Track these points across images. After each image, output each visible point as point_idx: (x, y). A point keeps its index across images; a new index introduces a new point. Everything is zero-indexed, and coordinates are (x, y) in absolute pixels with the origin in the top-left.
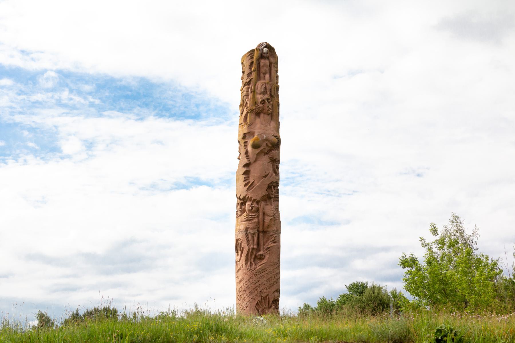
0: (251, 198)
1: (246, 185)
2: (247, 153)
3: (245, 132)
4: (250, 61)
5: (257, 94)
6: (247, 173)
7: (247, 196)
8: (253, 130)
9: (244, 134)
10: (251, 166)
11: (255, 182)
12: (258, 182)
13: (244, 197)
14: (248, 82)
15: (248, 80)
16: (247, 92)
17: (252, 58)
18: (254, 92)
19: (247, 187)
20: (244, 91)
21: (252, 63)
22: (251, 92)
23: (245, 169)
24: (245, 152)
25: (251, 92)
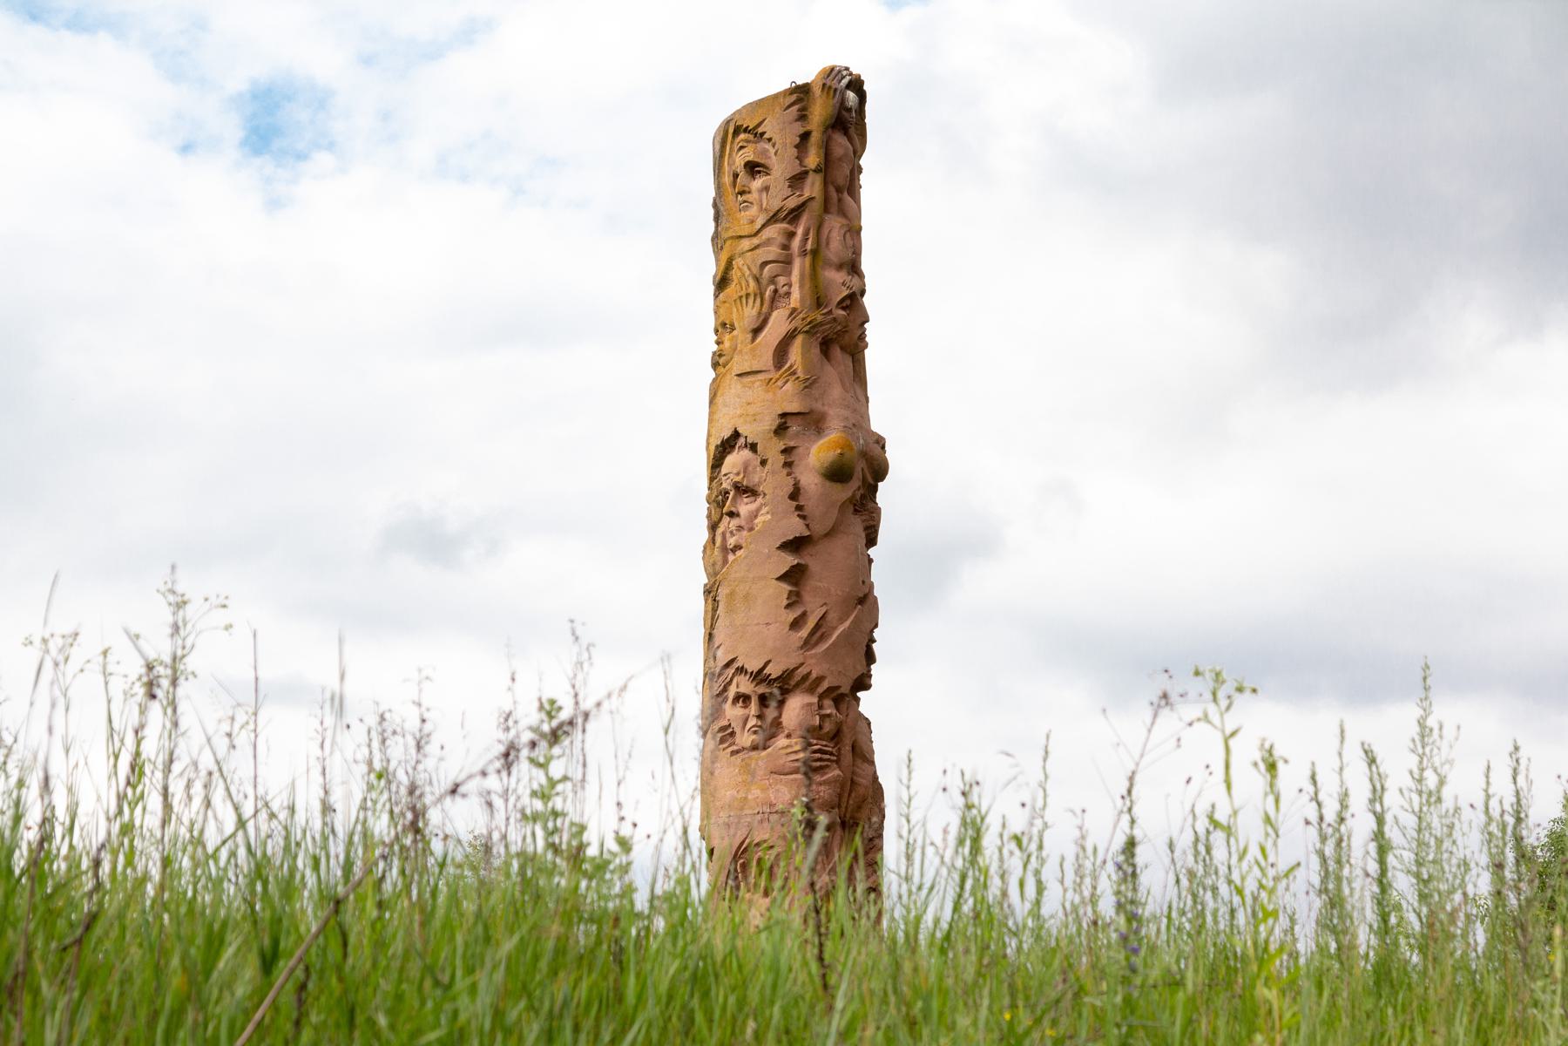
0: (820, 679)
1: (796, 624)
2: (795, 495)
3: (793, 407)
4: (799, 129)
6: (794, 576)
7: (802, 671)
8: (818, 406)
9: (784, 415)
10: (810, 550)
11: (830, 617)
13: (786, 676)
14: (793, 211)
15: (792, 203)
16: (786, 247)
17: (802, 117)
18: (815, 253)
19: (804, 633)
20: (768, 242)
21: (805, 136)
22: (804, 253)
23: (789, 560)
25: (804, 253)
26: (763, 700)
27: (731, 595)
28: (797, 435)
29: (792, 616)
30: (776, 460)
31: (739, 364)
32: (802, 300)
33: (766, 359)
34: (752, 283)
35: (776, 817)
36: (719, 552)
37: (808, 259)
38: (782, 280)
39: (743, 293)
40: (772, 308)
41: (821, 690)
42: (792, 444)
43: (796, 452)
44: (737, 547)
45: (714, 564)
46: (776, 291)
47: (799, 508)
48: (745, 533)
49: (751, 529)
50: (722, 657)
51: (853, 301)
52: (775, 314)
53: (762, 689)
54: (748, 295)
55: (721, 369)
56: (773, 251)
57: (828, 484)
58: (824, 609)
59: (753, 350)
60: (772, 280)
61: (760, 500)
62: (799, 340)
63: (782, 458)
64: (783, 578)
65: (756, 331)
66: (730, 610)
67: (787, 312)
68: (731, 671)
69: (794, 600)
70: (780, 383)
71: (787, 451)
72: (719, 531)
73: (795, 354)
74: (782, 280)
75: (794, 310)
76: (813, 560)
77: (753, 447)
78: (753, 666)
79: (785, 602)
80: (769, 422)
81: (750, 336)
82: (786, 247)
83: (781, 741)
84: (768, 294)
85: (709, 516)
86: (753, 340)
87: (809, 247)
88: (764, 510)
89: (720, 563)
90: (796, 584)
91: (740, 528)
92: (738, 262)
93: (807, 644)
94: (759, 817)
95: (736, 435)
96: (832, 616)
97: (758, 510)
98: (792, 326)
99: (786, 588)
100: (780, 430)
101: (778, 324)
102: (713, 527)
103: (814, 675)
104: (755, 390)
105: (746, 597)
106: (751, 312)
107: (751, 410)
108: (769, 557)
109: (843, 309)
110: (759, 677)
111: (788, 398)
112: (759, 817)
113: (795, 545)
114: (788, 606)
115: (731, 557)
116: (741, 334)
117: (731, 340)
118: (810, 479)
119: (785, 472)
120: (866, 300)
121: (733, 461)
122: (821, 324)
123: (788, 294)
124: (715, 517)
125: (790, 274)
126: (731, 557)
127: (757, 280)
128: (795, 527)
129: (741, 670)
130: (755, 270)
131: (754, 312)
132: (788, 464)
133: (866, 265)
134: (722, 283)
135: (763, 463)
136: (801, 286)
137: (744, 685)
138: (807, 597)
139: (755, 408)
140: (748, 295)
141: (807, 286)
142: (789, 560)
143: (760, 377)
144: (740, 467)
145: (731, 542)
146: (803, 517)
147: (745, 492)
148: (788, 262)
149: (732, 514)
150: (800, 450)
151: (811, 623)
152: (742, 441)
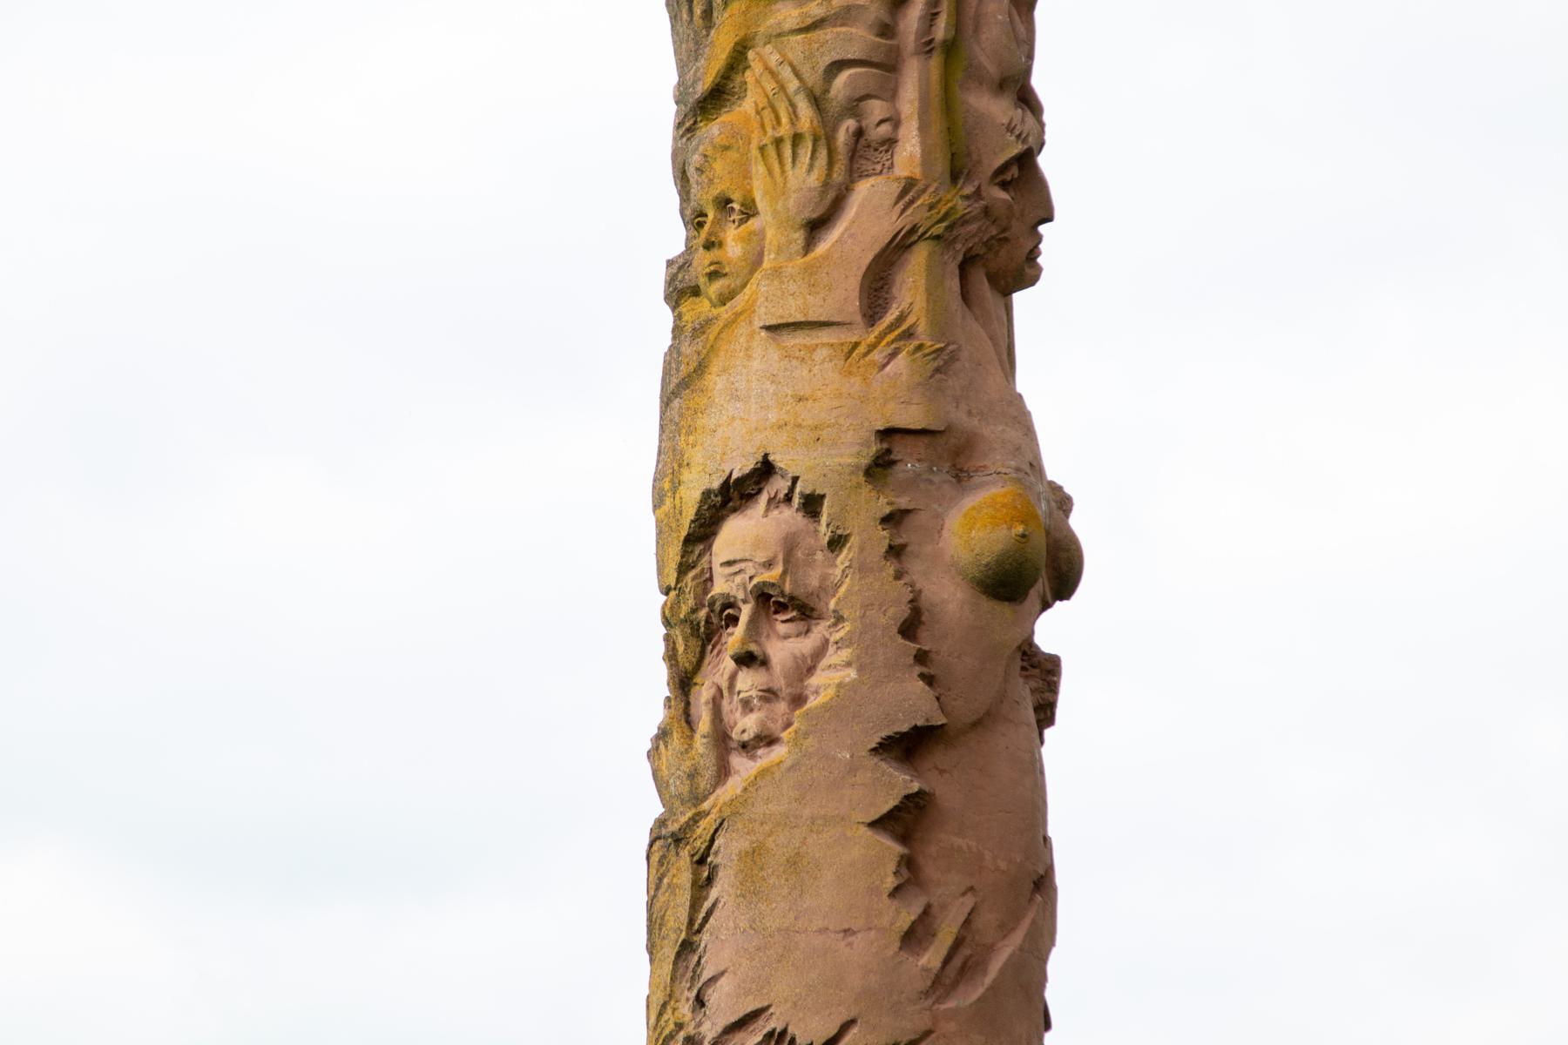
1: (914, 937)
2: (909, 628)
5: (975, 76)
6: (905, 821)
8: (959, 417)
9: (887, 434)
10: (939, 757)
11: (980, 922)
12: (1005, 929)
16: (886, 30)
18: (951, 48)
19: (932, 958)
22: (927, 48)
23: (899, 782)
24: (904, 612)
25: (927, 48)
27: (754, 855)
28: (912, 483)
29: (907, 917)
30: (867, 537)
31: (769, 298)
32: (926, 154)
33: (844, 295)
34: (805, 111)
36: (698, 743)
37: (936, 61)
38: (876, 109)
39: (785, 130)
40: (855, 174)
42: (904, 502)
43: (910, 521)
44: (767, 739)
45: (693, 775)
46: (859, 133)
47: (921, 658)
48: (782, 707)
49: (798, 700)
50: (724, 1005)
51: (1023, 174)
52: (863, 188)
54: (797, 139)
55: (700, 308)
56: (857, 39)
57: (987, 604)
58: (969, 901)
59: (809, 270)
60: (854, 107)
61: (820, 630)
62: (919, 257)
63: (883, 537)
64: (879, 824)
65: (816, 227)
66: (751, 890)
67: (896, 189)
69: (910, 874)
70: (877, 356)
71: (893, 519)
72: (703, 694)
73: (912, 289)
74: (876, 109)
75: (909, 184)
76: (942, 779)
77: (812, 505)
79: (890, 882)
80: (853, 450)
81: (799, 236)
82: (886, 30)
84: (842, 137)
85: (671, 656)
86: (809, 245)
87: (941, 30)
88: (833, 657)
89: (708, 774)
90: (904, 838)
91: (769, 695)
92: (763, 57)
93: (941, 984)
95: (766, 469)
96: (987, 920)
97: (820, 652)
98: (906, 221)
99: (892, 848)
100: (879, 468)
101: (871, 213)
102: (683, 683)
104: (818, 370)
105: (794, 863)
106: (804, 177)
107: (809, 414)
108: (852, 769)
109: (1004, 185)
111: (895, 392)
113: (907, 746)
114: (896, 892)
115: (738, 761)
116: (774, 223)
117: (746, 239)
118: (949, 596)
119: (890, 568)
120: (1044, 161)
121: (746, 536)
122: (964, 221)
123: (890, 142)
124: (685, 661)
125: (892, 95)
126: (738, 761)
127: (817, 101)
128: (912, 703)
130: (813, 78)
131: (814, 180)
132: (895, 552)
133: (1040, 82)
134: (704, 103)
135: (836, 543)
136: (923, 128)
138: (930, 870)
139: (799, 405)
140: (797, 139)
141: (937, 127)
142: (899, 782)
143: (825, 336)
144: (774, 548)
145: (746, 725)
146: (929, 680)
147: (781, 607)
148: (889, 66)
149: (746, 660)
150: (921, 518)
151: (946, 933)
152: (779, 485)
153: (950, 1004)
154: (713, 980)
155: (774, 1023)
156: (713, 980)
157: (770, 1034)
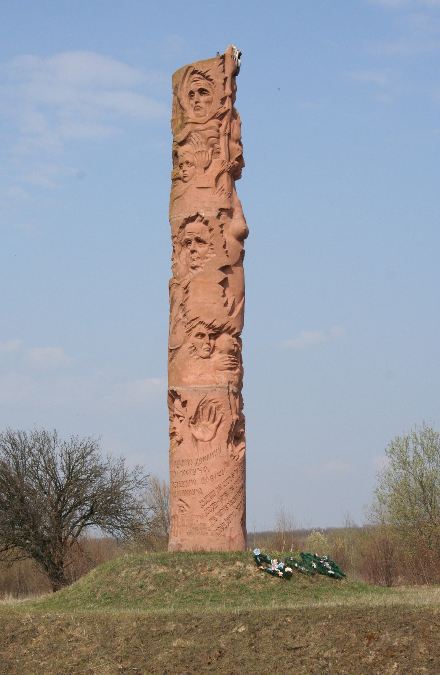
0: (234, 329)
1: (226, 305)
23: (222, 276)
26: (210, 335)
35: (219, 389)
41: (233, 334)
53: (211, 332)
68: (195, 323)
78: (208, 321)
83: (216, 356)
90: (222, 286)
94: (211, 389)
103: (232, 328)
110: (209, 327)
112: (211, 389)
129: (201, 323)
137: (203, 329)
142: (222, 276)
153: (232, 317)
154: (188, 311)
155: (201, 320)
156: (188, 311)
157: (200, 322)
